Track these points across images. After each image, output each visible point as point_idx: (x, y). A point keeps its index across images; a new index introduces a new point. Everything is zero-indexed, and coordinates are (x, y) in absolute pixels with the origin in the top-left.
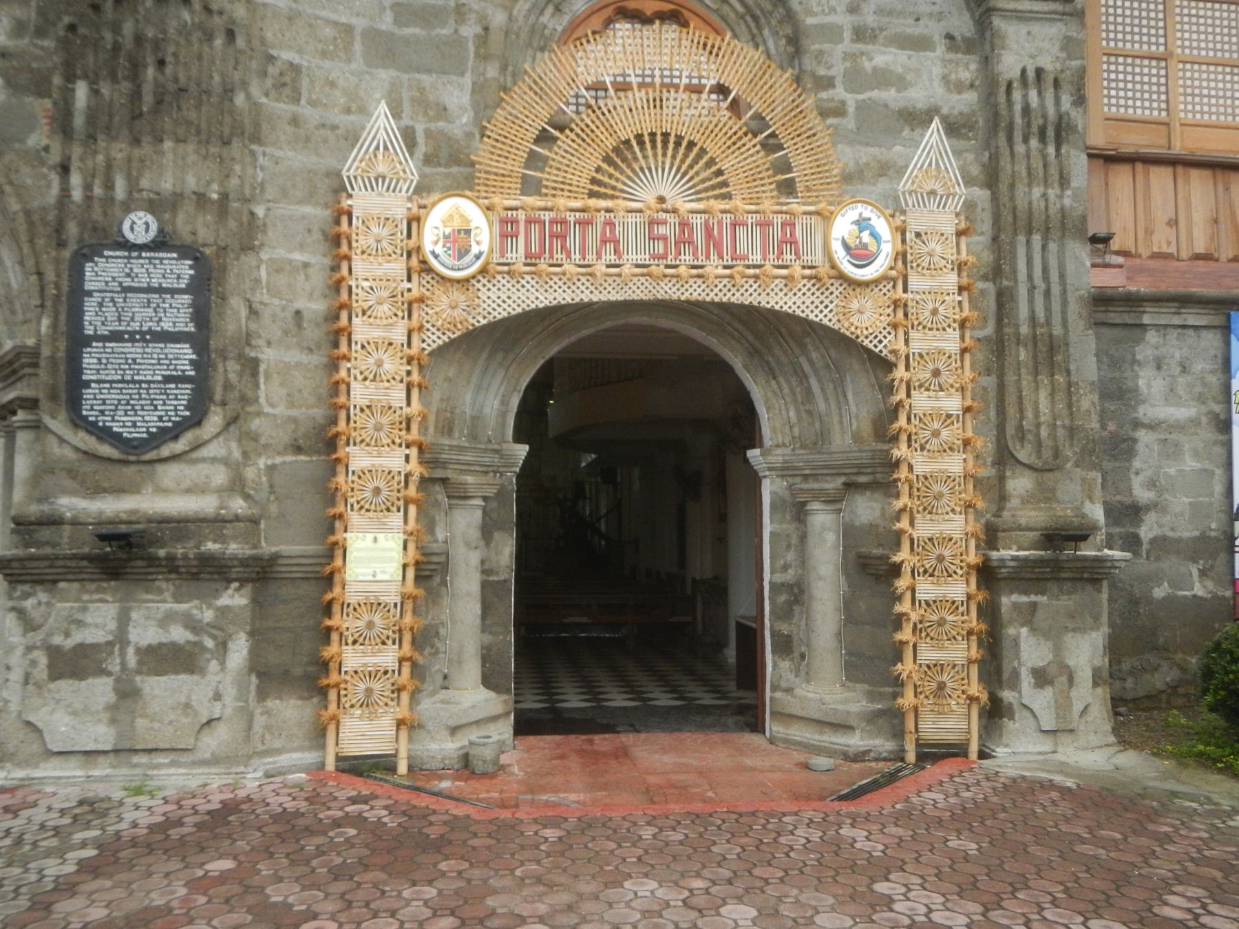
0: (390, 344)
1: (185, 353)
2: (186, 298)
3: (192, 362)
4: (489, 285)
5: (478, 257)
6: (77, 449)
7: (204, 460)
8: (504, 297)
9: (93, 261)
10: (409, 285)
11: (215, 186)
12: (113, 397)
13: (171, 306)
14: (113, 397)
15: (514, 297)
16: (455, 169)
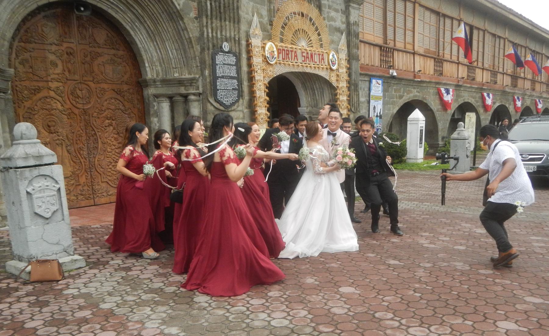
1: (235, 81)
7: (238, 111)
12: (223, 94)
14: (223, 94)
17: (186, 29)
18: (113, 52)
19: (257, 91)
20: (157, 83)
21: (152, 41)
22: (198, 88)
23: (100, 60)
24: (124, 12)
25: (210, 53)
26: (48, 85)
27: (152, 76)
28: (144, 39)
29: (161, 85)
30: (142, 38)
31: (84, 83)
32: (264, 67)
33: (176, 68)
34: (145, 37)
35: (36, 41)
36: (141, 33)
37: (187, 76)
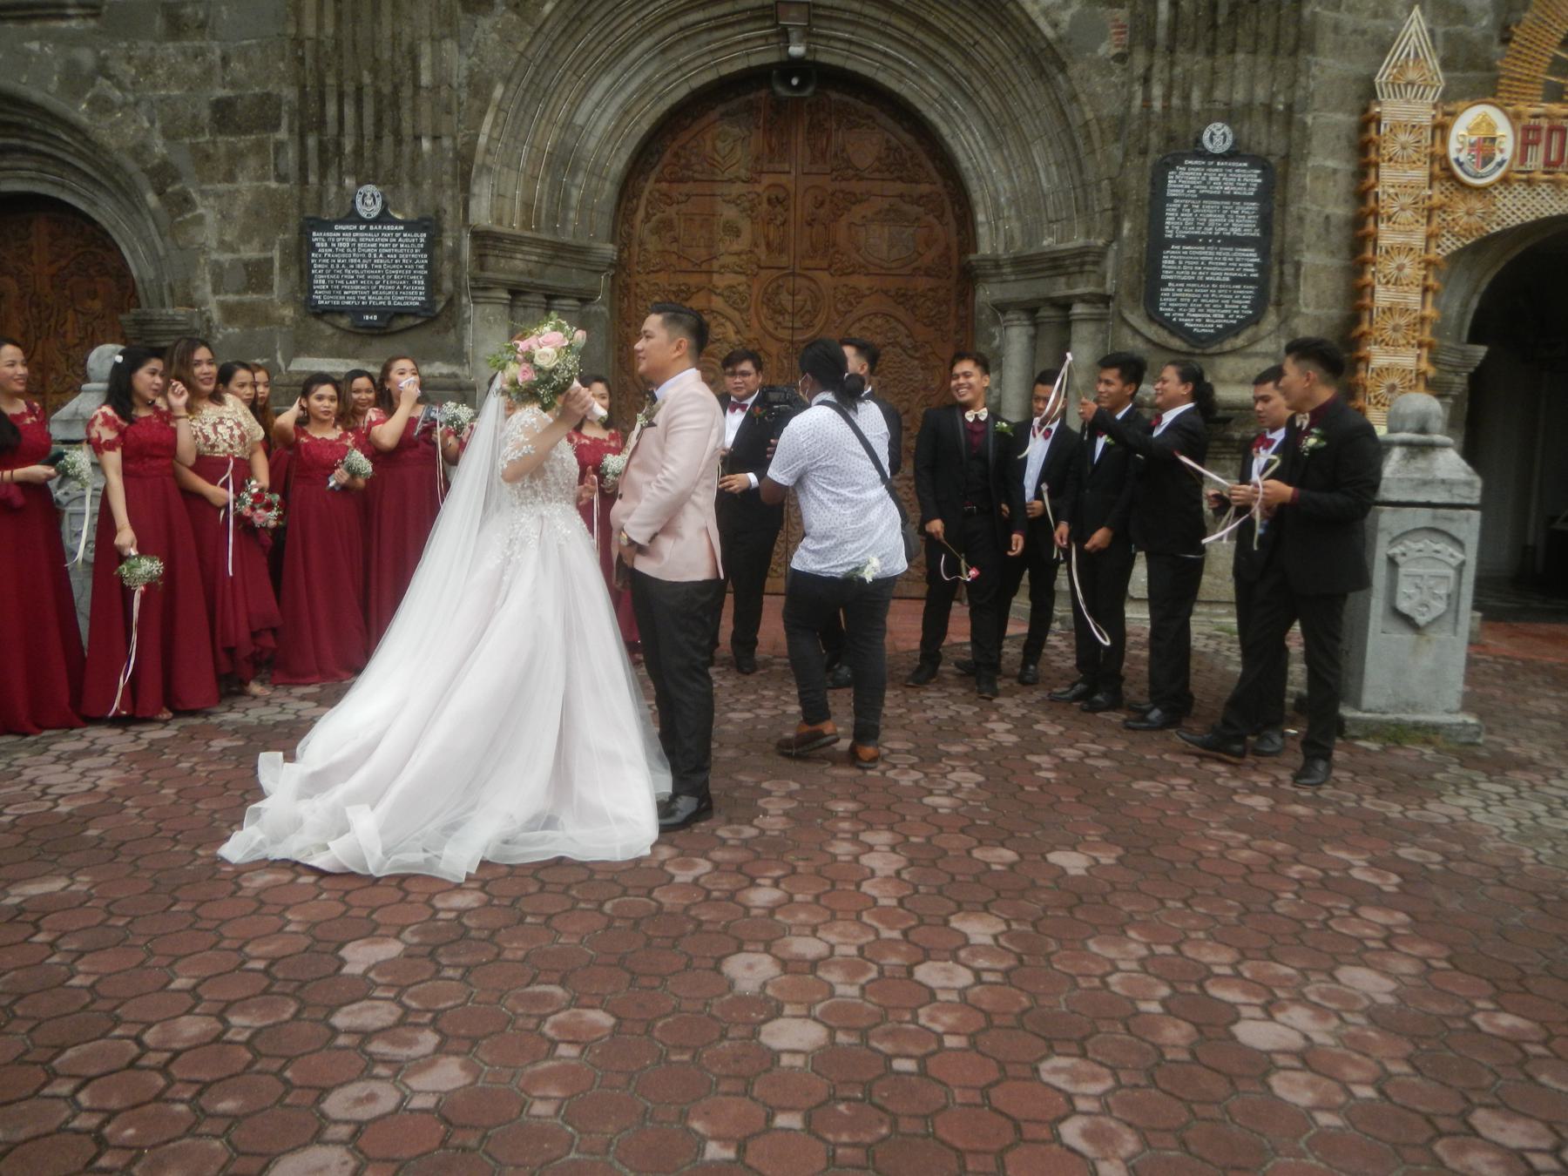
0: (1411, 249)
1: (1251, 255)
2: (1254, 205)
3: (1256, 265)
4: (1506, 193)
5: (1500, 164)
6: (1148, 340)
7: (1256, 354)
8: (1519, 204)
9: (1174, 169)
10: (1429, 193)
11: (1281, 98)
12: (1187, 295)
13: (1240, 214)
14: (1187, 295)
15: (1529, 205)
16: (1471, 74)
17: (1074, 98)
18: (900, 187)
19: (1379, 289)
20: (1004, 271)
21: (999, 146)
22: (1102, 281)
23: (858, 212)
24: (921, 76)
25: (1149, 163)
26: (710, 281)
27: (995, 249)
28: (977, 142)
29: (1013, 273)
30: (972, 141)
31: (805, 276)
32: (1438, 198)
33: (1057, 221)
34: (979, 138)
35: (697, 176)
36: (969, 127)
37: (1078, 241)
